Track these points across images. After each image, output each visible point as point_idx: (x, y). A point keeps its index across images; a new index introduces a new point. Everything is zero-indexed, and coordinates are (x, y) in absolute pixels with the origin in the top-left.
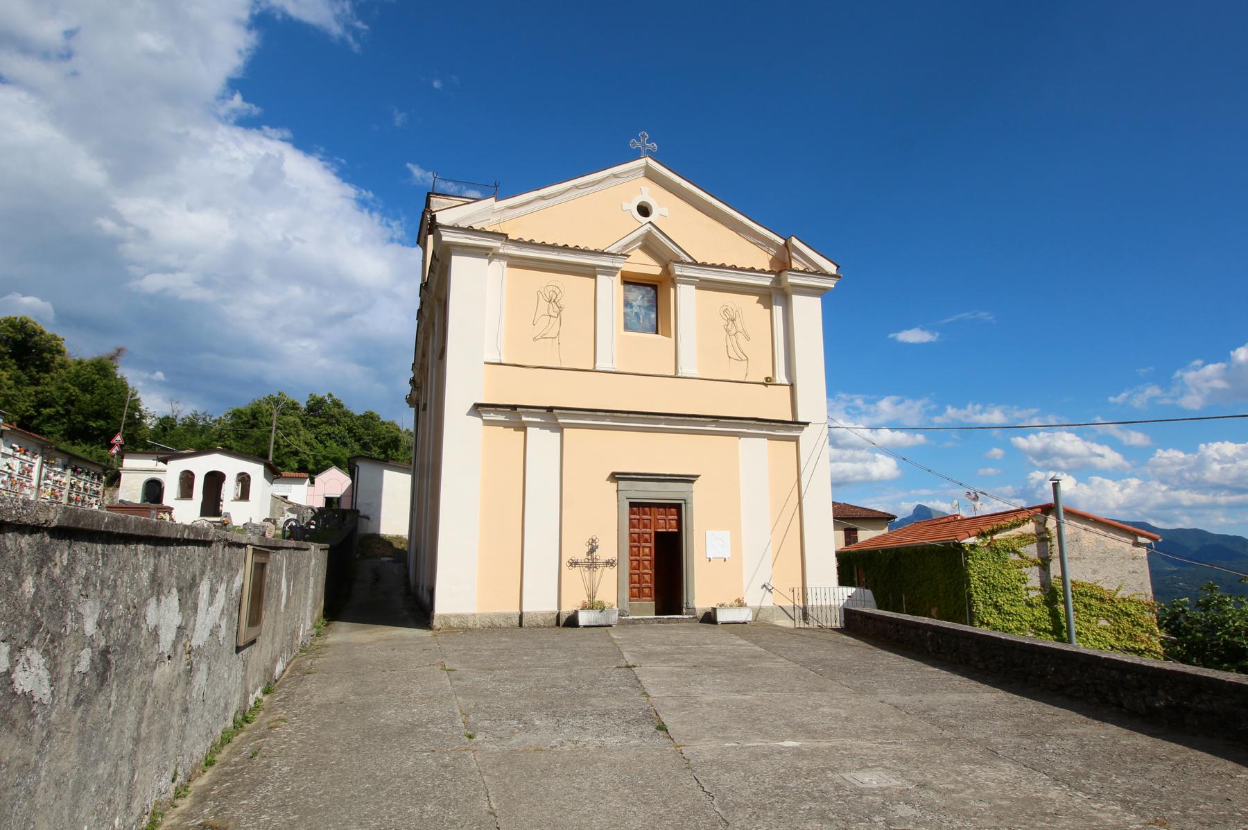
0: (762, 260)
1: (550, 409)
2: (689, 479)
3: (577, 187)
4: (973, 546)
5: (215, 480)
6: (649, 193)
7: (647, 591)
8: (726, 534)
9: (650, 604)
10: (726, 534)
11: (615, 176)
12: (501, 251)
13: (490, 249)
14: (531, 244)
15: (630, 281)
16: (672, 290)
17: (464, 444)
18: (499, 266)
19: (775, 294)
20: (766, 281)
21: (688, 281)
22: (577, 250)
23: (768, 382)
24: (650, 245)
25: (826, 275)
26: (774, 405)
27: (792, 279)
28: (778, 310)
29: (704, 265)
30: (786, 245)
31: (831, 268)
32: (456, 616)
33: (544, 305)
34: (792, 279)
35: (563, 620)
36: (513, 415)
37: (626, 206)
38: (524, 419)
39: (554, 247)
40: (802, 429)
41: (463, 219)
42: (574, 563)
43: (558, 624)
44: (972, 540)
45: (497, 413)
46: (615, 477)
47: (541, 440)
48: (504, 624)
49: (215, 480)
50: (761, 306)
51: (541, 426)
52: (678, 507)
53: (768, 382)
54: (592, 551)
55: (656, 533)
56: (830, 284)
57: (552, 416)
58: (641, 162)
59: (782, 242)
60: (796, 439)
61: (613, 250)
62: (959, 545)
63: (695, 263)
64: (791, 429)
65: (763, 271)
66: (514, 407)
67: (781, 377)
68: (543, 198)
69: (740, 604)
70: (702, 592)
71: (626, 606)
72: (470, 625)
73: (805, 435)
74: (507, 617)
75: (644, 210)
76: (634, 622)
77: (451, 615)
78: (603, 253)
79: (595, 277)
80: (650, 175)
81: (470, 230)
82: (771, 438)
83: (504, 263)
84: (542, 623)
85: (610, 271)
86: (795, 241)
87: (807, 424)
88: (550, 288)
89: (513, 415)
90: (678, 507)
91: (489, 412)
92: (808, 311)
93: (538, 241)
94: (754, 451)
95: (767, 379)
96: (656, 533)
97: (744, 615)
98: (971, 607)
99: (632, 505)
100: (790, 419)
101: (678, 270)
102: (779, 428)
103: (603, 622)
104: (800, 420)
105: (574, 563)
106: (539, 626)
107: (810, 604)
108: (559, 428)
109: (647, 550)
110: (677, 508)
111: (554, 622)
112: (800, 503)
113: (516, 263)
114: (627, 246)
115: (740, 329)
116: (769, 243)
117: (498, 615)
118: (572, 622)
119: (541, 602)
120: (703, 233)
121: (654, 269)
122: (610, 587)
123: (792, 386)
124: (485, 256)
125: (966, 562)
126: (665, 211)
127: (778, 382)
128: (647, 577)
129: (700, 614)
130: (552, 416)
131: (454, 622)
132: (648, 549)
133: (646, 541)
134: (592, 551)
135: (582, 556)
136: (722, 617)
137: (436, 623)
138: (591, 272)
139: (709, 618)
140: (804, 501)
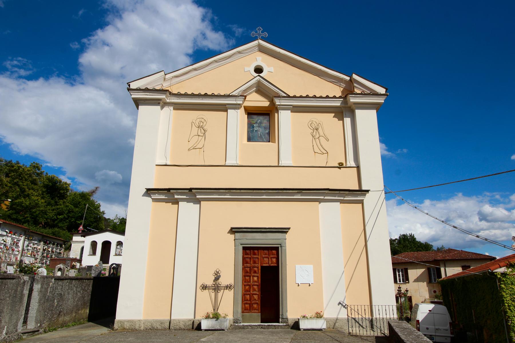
0: (337, 91)
1: (190, 190)
2: (284, 231)
3: (216, 61)
4: (504, 274)
5: (107, 245)
6: (261, 60)
7: (255, 306)
8: (310, 268)
9: (257, 315)
10: (310, 268)
11: (239, 52)
12: (168, 101)
13: (160, 100)
14: (186, 95)
15: (251, 113)
16: (276, 114)
17: (139, 212)
18: (168, 110)
19: (345, 111)
20: (337, 103)
21: (286, 108)
22: (213, 96)
23: (341, 166)
24: (261, 89)
25: (376, 94)
26: (346, 180)
27: (353, 100)
28: (348, 121)
29: (295, 97)
30: (350, 80)
31: (382, 91)
32: (128, 321)
33: (195, 130)
34: (353, 100)
35: (196, 325)
36: (169, 195)
37: (247, 69)
38: (176, 197)
39: (199, 96)
40: (365, 195)
41: (148, 84)
42: (204, 287)
43: (193, 328)
44: (502, 270)
45: (160, 194)
46: (234, 231)
47: (187, 209)
48: (159, 327)
49: (107, 245)
50: (336, 119)
51: (188, 201)
52: (277, 249)
53: (341, 166)
54: (217, 278)
55: (262, 267)
56: (381, 100)
57: (192, 194)
58: (255, 43)
59: (348, 78)
60: (362, 202)
61: (234, 94)
62: (492, 274)
63: (289, 96)
64: (357, 195)
65: (335, 97)
66: (169, 190)
67: (351, 162)
68: (195, 69)
69: (319, 316)
70: (293, 308)
71: (239, 316)
72: (137, 327)
73: (367, 199)
74: (162, 322)
75: (259, 70)
76: (244, 327)
77: (125, 321)
78: (229, 96)
79: (227, 111)
80: (262, 50)
81: (147, 90)
82: (342, 202)
83: (172, 108)
84: (183, 327)
85: (236, 107)
86: (355, 76)
87: (368, 191)
88: (198, 120)
89: (169, 195)
90: (277, 249)
91: (155, 194)
92: (367, 121)
93: (189, 93)
94: (330, 212)
95: (339, 164)
96: (262, 267)
97: (320, 324)
98: (507, 321)
99: (244, 249)
100: (358, 189)
101: (278, 102)
102: (348, 195)
103: (218, 327)
104: (363, 189)
105: (204, 287)
106: (180, 329)
107: (374, 317)
108: (198, 201)
109: (256, 279)
110: (275, 251)
111: (191, 326)
112: (366, 245)
113: (178, 107)
114: (245, 91)
115: (322, 134)
116: (341, 80)
117: (156, 321)
118: (199, 328)
119: (183, 312)
120: (290, 77)
121: (265, 103)
122: (229, 305)
123: (358, 167)
124: (158, 104)
125: (500, 287)
126: (272, 69)
127: (348, 165)
128: (256, 297)
129: (291, 323)
130: (192, 194)
131: (127, 326)
132: (256, 279)
133: (255, 272)
134: (217, 278)
135: (210, 282)
136: (304, 325)
137: (116, 326)
138: (224, 108)
139: (296, 326)
140: (368, 243)
